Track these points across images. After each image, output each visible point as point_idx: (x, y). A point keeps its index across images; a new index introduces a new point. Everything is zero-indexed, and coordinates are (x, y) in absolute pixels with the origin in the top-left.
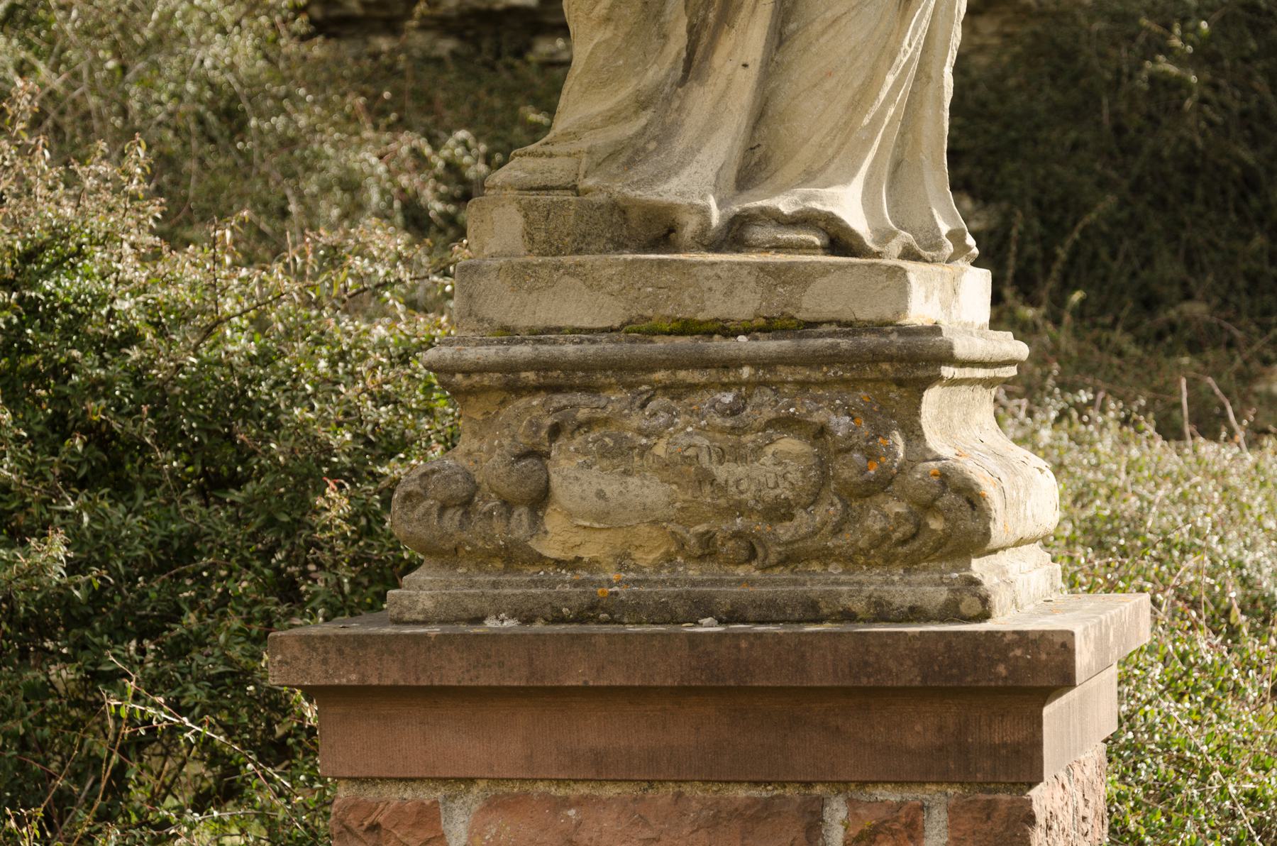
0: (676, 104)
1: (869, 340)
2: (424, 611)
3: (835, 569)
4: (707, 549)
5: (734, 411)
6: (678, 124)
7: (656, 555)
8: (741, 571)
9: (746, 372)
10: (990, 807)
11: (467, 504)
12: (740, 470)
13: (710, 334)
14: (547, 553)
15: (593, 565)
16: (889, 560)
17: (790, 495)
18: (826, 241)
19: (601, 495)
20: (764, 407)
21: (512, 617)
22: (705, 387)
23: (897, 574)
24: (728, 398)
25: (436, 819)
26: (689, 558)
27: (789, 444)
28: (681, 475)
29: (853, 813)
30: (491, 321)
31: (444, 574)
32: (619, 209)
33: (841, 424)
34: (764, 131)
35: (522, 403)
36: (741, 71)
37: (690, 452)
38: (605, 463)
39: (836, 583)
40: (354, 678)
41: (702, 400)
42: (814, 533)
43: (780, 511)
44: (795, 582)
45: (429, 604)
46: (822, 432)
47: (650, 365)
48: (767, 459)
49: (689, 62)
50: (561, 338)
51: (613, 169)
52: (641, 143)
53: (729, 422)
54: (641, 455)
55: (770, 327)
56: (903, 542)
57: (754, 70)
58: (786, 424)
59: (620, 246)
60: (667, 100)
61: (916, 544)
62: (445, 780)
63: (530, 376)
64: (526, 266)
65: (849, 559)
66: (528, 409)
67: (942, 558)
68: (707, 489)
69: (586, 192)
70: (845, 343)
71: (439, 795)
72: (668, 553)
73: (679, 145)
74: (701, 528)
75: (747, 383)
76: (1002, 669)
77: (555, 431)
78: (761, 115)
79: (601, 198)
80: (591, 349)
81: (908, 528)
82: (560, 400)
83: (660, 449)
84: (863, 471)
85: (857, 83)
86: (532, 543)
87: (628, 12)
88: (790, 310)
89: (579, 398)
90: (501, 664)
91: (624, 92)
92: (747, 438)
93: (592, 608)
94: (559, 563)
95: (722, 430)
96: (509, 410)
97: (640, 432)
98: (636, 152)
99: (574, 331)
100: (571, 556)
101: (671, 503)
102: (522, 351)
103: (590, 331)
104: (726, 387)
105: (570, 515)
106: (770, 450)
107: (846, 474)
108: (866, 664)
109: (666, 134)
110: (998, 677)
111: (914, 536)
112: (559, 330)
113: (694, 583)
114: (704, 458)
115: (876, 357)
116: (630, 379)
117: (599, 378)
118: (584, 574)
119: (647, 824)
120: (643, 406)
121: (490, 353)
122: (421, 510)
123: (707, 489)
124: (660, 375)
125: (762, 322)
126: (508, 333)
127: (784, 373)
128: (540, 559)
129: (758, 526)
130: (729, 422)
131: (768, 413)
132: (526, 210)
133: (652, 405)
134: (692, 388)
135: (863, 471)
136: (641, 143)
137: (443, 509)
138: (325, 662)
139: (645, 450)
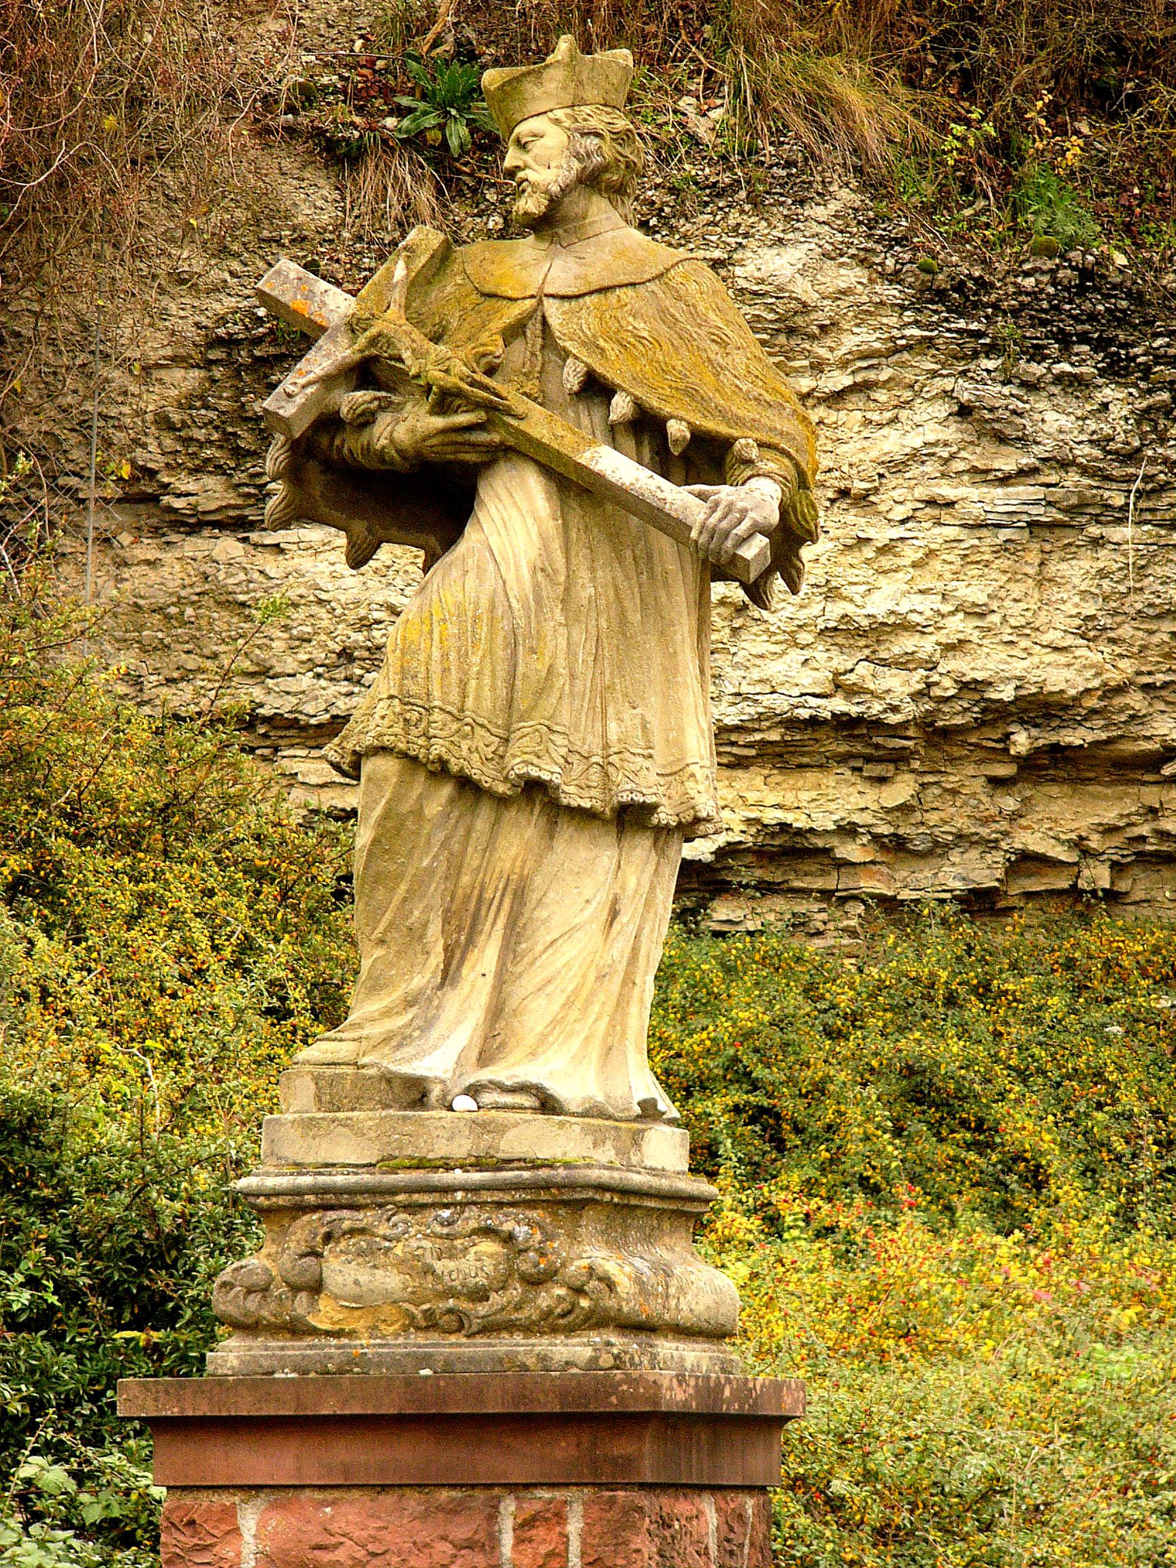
0: (436, 1003)
1: (543, 1173)
2: (232, 1368)
3: (518, 1338)
4: (431, 1324)
5: (450, 1223)
6: (436, 1017)
7: (396, 1327)
8: (453, 1339)
9: (459, 1196)
10: (612, 1502)
11: (265, 1289)
12: (452, 1265)
13: (436, 1168)
14: (319, 1326)
15: (351, 1334)
16: (554, 1330)
17: (485, 1282)
18: (537, 1104)
19: (356, 1282)
20: (472, 1219)
21: (293, 1371)
22: (433, 1205)
23: (561, 1338)
24: (446, 1213)
25: (234, 1516)
26: (418, 1328)
27: (488, 1246)
28: (412, 1268)
29: (519, 1508)
30: (286, 1158)
31: (249, 1342)
32: (388, 1079)
33: (521, 1231)
34: (501, 1024)
35: (306, 1218)
36: (481, 979)
37: (420, 1252)
38: (360, 1260)
39: (517, 1345)
40: (176, 1412)
41: (430, 1215)
42: (503, 1309)
43: (479, 1295)
44: (489, 1345)
45: (235, 1363)
46: (509, 1238)
47: (393, 1191)
48: (471, 1256)
49: (445, 972)
50: (334, 1171)
51: (387, 1050)
52: (408, 1031)
53: (445, 1231)
54: (385, 1254)
55: (479, 1165)
56: (563, 1315)
57: (490, 978)
58: (487, 1232)
59: (386, 1106)
60: (430, 1000)
61: (571, 1318)
62: (241, 1488)
63: (311, 1199)
64: (312, 1119)
65: (528, 1329)
66: (309, 1222)
67: (591, 1328)
68: (430, 1278)
69: (363, 1067)
70: (526, 1174)
71: (237, 1499)
72: (404, 1325)
73: (435, 1033)
74: (425, 1307)
75: (460, 1204)
76: (614, 1399)
77: (328, 1238)
78: (497, 1011)
79: (372, 1072)
80: (352, 1179)
81: (565, 1306)
82: (332, 1215)
83: (399, 1250)
84: (536, 1265)
85: (571, 988)
86: (310, 1319)
87: (396, 935)
88: (492, 1152)
89: (345, 1213)
90: (277, 1400)
91: (394, 996)
92: (458, 1242)
93: (348, 1363)
94: (328, 1333)
95: (441, 1237)
96: (299, 1223)
97: (385, 1238)
98: (405, 1038)
99: (344, 1166)
100: (337, 1327)
101: (405, 1288)
102: (305, 1181)
103: (356, 1166)
104: (446, 1206)
105: (336, 1297)
106: (472, 1250)
107: (524, 1267)
108: (525, 1397)
109: (427, 1025)
110: (612, 1405)
111: (570, 1312)
112: (334, 1165)
113: (420, 1346)
114: (428, 1255)
115: (547, 1186)
116: (381, 1200)
117: (360, 1200)
118: (345, 1341)
119: (379, 1518)
120: (389, 1220)
121: (284, 1182)
122: (232, 1293)
123: (430, 1278)
124: (400, 1198)
125: (473, 1160)
126: (299, 1168)
127: (486, 1196)
128: (314, 1332)
129: (464, 1305)
130: (445, 1231)
131: (473, 1224)
132: (317, 1079)
133: (394, 1219)
134: (423, 1206)
135: (536, 1265)
136: (408, 1031)
137: (249, 1292)
138: (156, 1400)
139: (389, 1249)
